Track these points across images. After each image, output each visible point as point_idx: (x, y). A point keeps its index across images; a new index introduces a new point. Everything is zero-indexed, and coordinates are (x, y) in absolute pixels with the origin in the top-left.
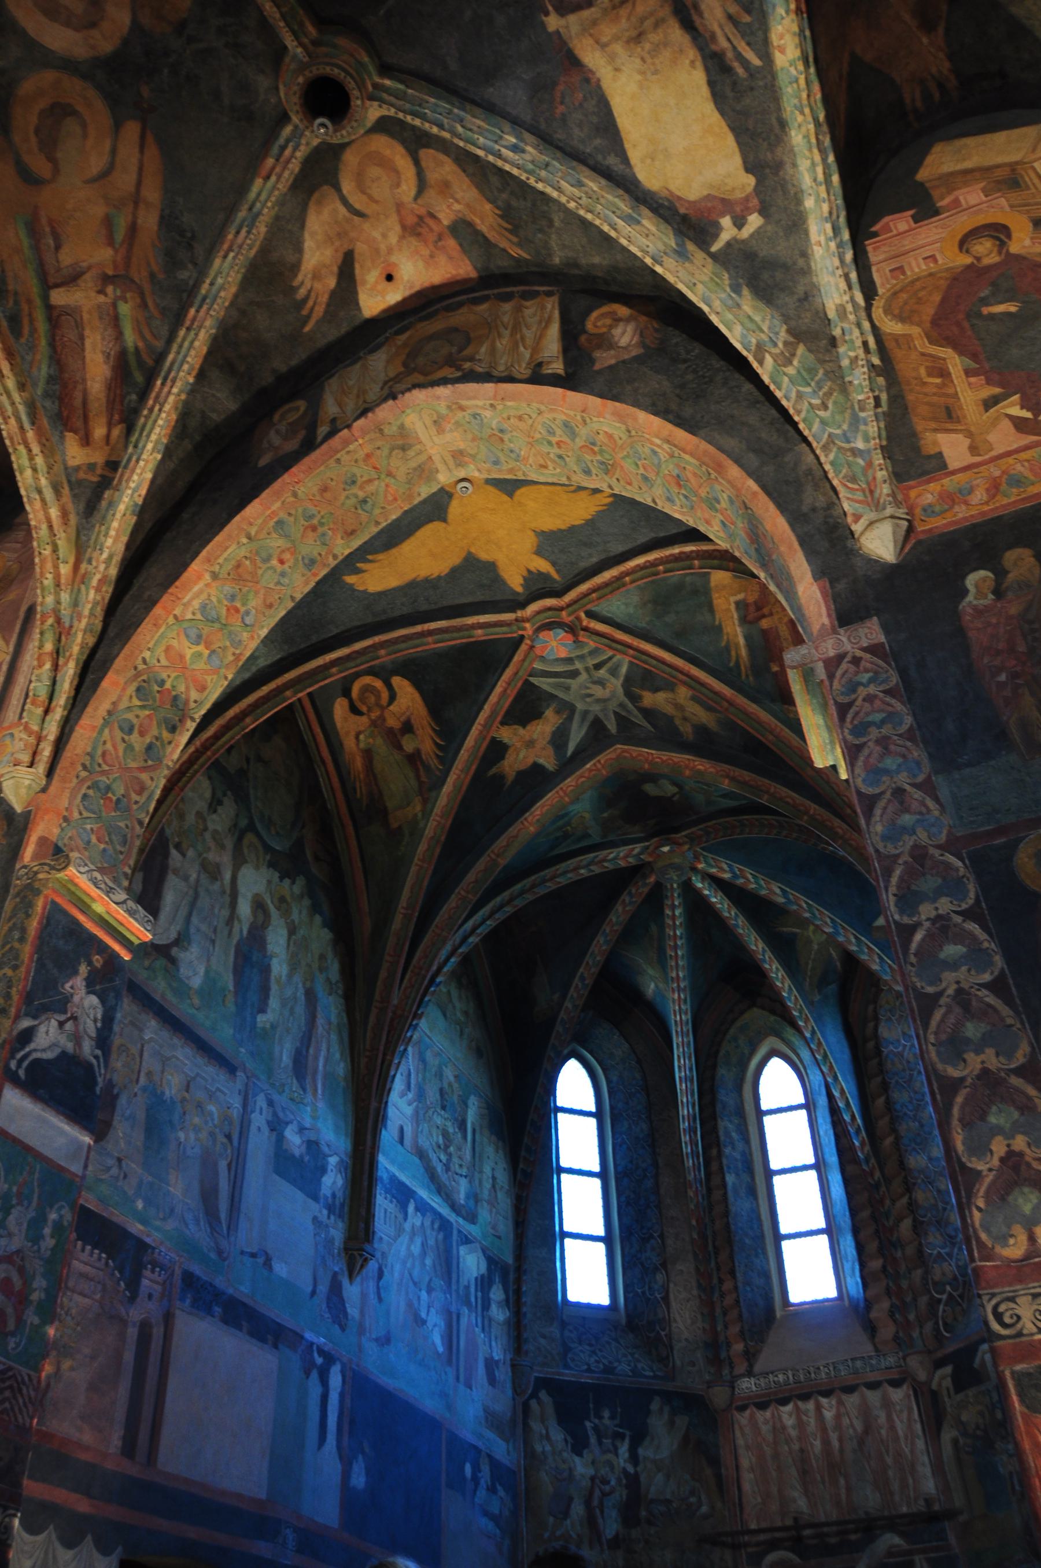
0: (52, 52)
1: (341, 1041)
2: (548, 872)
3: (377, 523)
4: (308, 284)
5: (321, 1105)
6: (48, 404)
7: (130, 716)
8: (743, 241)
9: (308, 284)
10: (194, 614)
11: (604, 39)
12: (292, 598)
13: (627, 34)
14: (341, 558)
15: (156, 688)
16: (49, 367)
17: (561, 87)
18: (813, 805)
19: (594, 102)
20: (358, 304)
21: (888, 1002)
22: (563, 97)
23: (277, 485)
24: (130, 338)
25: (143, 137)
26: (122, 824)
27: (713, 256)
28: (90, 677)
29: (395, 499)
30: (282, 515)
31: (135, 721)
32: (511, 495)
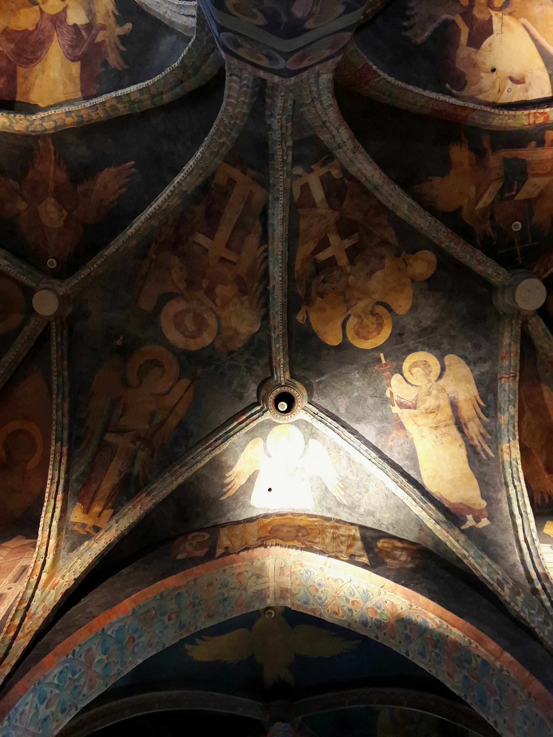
3: (226, 616)
4: (232, 478)
6: (75, 485)
7: (47, 689)
8: (479, 529)
9: (232, 478)
10: (112, 633)
11: (419, 424)
12: (164, 645)
13: (431, 425)
14: (199, 629)
15: (70, 676)
16: (86, 467)
17: (393, 435)
19: (408, 446)
23: (187, 571)
24: (137, 469)
27: (463, 532)
28: (34, 652)
29: (241, 605)
30: (183, 590)
31: (49, 696)
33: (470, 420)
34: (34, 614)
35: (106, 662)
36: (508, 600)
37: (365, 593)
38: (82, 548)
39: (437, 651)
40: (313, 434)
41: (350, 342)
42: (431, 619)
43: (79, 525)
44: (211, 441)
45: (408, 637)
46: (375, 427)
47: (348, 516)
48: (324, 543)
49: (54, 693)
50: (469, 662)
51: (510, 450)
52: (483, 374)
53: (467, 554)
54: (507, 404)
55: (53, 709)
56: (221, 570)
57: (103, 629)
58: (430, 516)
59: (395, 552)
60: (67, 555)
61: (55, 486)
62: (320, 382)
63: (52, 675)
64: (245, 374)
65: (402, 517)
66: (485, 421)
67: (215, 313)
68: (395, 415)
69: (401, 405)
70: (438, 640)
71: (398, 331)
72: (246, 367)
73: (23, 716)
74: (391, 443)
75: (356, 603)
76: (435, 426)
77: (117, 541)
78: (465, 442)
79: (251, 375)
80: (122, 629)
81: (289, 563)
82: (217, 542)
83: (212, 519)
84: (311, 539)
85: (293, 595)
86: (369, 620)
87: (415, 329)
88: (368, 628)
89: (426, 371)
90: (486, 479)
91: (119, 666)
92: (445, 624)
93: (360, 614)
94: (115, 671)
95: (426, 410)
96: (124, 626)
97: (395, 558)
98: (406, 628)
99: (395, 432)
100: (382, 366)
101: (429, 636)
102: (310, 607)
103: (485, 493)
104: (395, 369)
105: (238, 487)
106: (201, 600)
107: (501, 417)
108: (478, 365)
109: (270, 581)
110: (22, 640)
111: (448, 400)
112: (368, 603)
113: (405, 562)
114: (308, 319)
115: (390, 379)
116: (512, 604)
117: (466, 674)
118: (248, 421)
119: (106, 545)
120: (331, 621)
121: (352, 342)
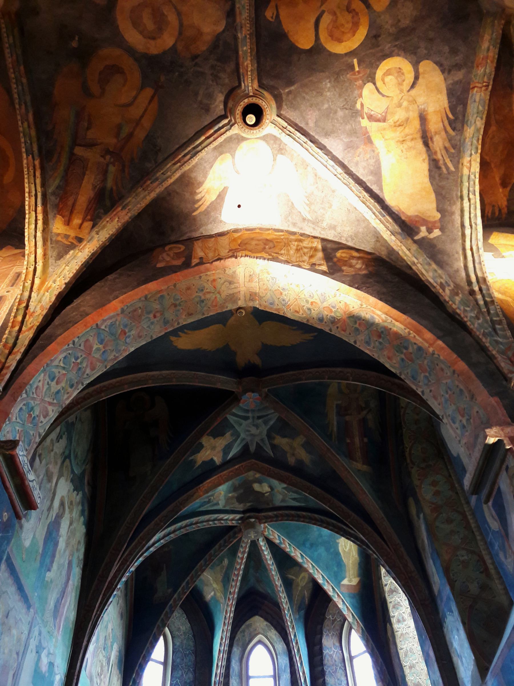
0: (127, 42)
1: (76, 596)
2: (194, 520)
3: (203, 314)
4: (202, 194)
5: (60, 638)
8: (430, 239)
9: (202, 194)
10: (106, 327)
11: (386, 137)
13: (398, 139)
15: (73, 360)
17: (360, 150)
18: (353, 514)
19: (374, 161)
20: (221, 212)
21: (328, 626)
22: (360, 154)
23: (167, 278)
24: (110, 183)
25: (153, 97)
26: (31, 433)
27: (415, 242)
28: (39, 342)
29: (216, 306)
30: (165, 293)
31: (57, 374)
32: (260, 322)
33: (436, 133)
34: (34, 312)
35: (104, 350)
36: (447, 299)
37: (322, 295)
38: (68, 256)
39: (381, 340)
40: (281, 149)
41: (323, 46)
42: (378, 315)
43: (63, 236)
44: (180, 156)
45: (357, 330)
46: (344, 141)
47: (312, 230)
48: (288, 254)
49: (61, 373)
50: (406, 348)
51: (470, 165)
52: (455, 83)
53: (416, 261)
54: (475, 116)
55: (63, 384)
56: (197, 277)
57: (97, 324)
58: (387, 228)
59: (352, 261)
60: (56, 262)
61: (33, 199)
62: (290, 92)
63: (58, 360)
64: (211, 82)
65: (361, 230)
66: (450, 135)
67: (175, 8)
68: (364, 129)
69: (371, 118)
70: (382, 332)
71: (374, 32)
72: (212, 74)
73: (38, 390)
74: (357, 158)
75: (314, 304)
76: (401, 139)
77: (100, 251)
78: (429, 156)
79: (217, 84)
80: (114, 324)
81: (257, 271)
82: (192, 253)
83: (186, 233)
84: (276, 250)
85: (261, 298)
86: (324, 317)
87: (392, 30)
88: (324, 323)
89: (399, 80)
90: (444, 192)
91: (114, 353)
92: (390, 319)
93: (317, 312)
94: (112, 357)
95: (395, 123)
96: (115, 322)
97: (351, 266)
98: (356, 322)
99: (362, 146)
100: (354, 74)
101: (375, 329)
102: (275, 307)
103: (441, 206)
104: (368, 77)
105: (209, 203)
106: (182, 302)
107: (466, 130)
108: (452, 72)
109: (241, 286)
110: (27, 333)
111: (417, 112)
112: (325, 303)
113: (360, 269)
114: (278, 16)
115: (361, 88)
116: (450, 303)
117: (403, 356)
118: (215, 136)
119: (90, 254)
120: (292, 318)
121: (324, 45)
